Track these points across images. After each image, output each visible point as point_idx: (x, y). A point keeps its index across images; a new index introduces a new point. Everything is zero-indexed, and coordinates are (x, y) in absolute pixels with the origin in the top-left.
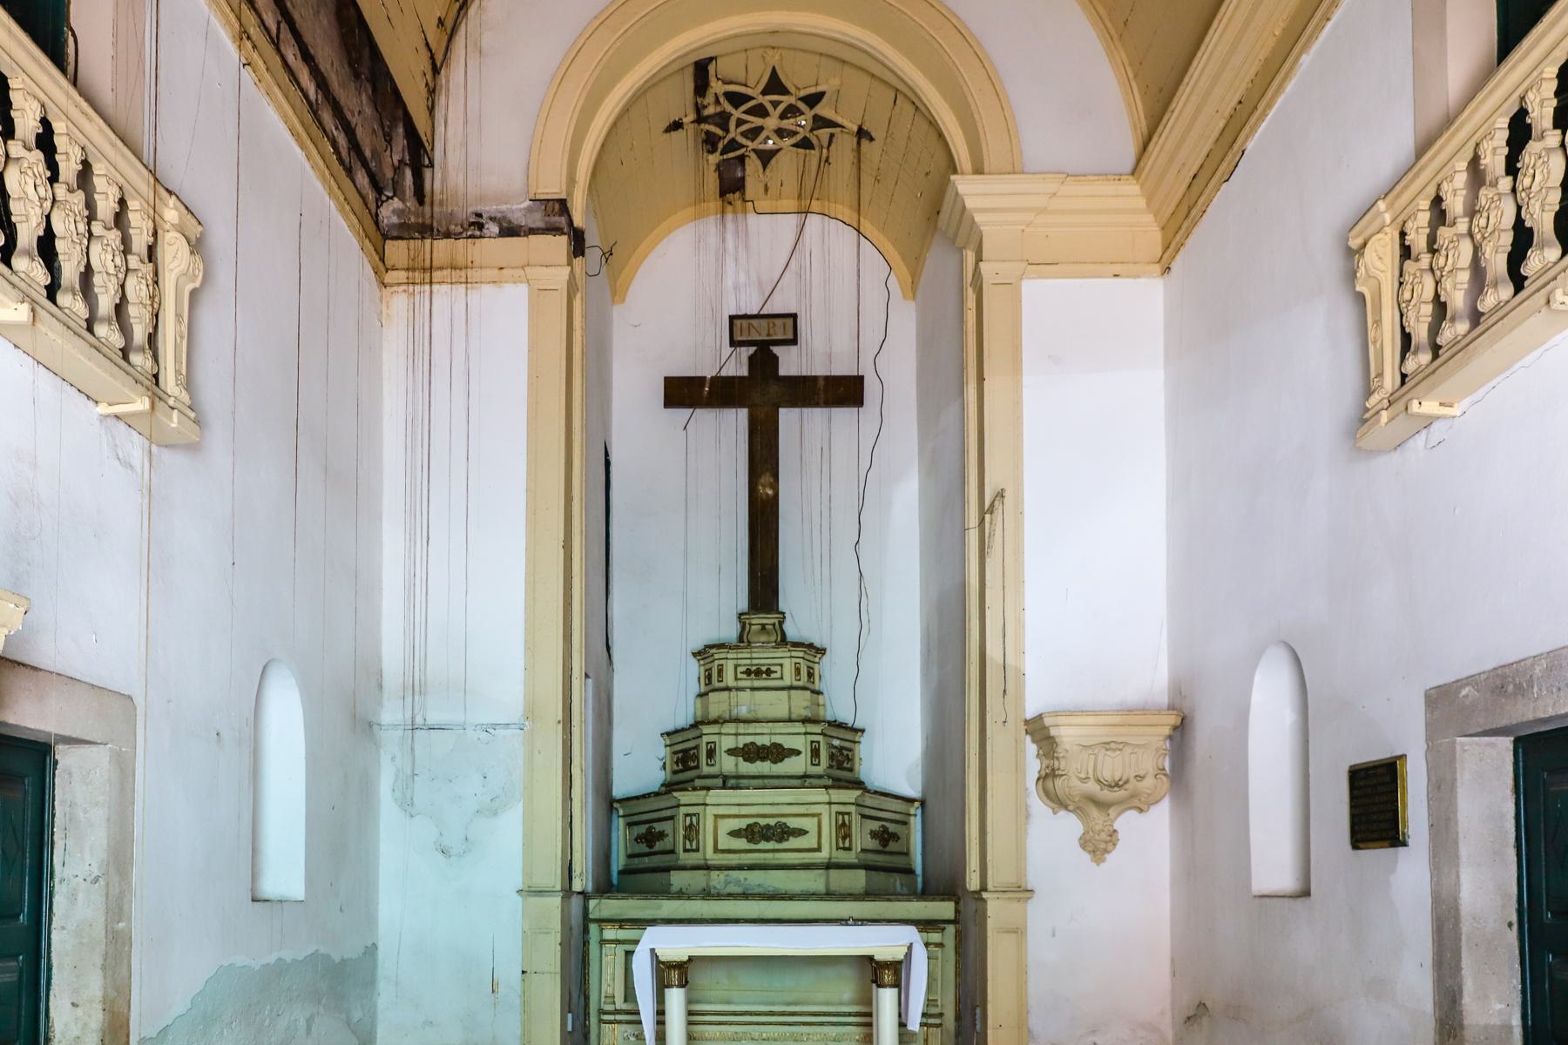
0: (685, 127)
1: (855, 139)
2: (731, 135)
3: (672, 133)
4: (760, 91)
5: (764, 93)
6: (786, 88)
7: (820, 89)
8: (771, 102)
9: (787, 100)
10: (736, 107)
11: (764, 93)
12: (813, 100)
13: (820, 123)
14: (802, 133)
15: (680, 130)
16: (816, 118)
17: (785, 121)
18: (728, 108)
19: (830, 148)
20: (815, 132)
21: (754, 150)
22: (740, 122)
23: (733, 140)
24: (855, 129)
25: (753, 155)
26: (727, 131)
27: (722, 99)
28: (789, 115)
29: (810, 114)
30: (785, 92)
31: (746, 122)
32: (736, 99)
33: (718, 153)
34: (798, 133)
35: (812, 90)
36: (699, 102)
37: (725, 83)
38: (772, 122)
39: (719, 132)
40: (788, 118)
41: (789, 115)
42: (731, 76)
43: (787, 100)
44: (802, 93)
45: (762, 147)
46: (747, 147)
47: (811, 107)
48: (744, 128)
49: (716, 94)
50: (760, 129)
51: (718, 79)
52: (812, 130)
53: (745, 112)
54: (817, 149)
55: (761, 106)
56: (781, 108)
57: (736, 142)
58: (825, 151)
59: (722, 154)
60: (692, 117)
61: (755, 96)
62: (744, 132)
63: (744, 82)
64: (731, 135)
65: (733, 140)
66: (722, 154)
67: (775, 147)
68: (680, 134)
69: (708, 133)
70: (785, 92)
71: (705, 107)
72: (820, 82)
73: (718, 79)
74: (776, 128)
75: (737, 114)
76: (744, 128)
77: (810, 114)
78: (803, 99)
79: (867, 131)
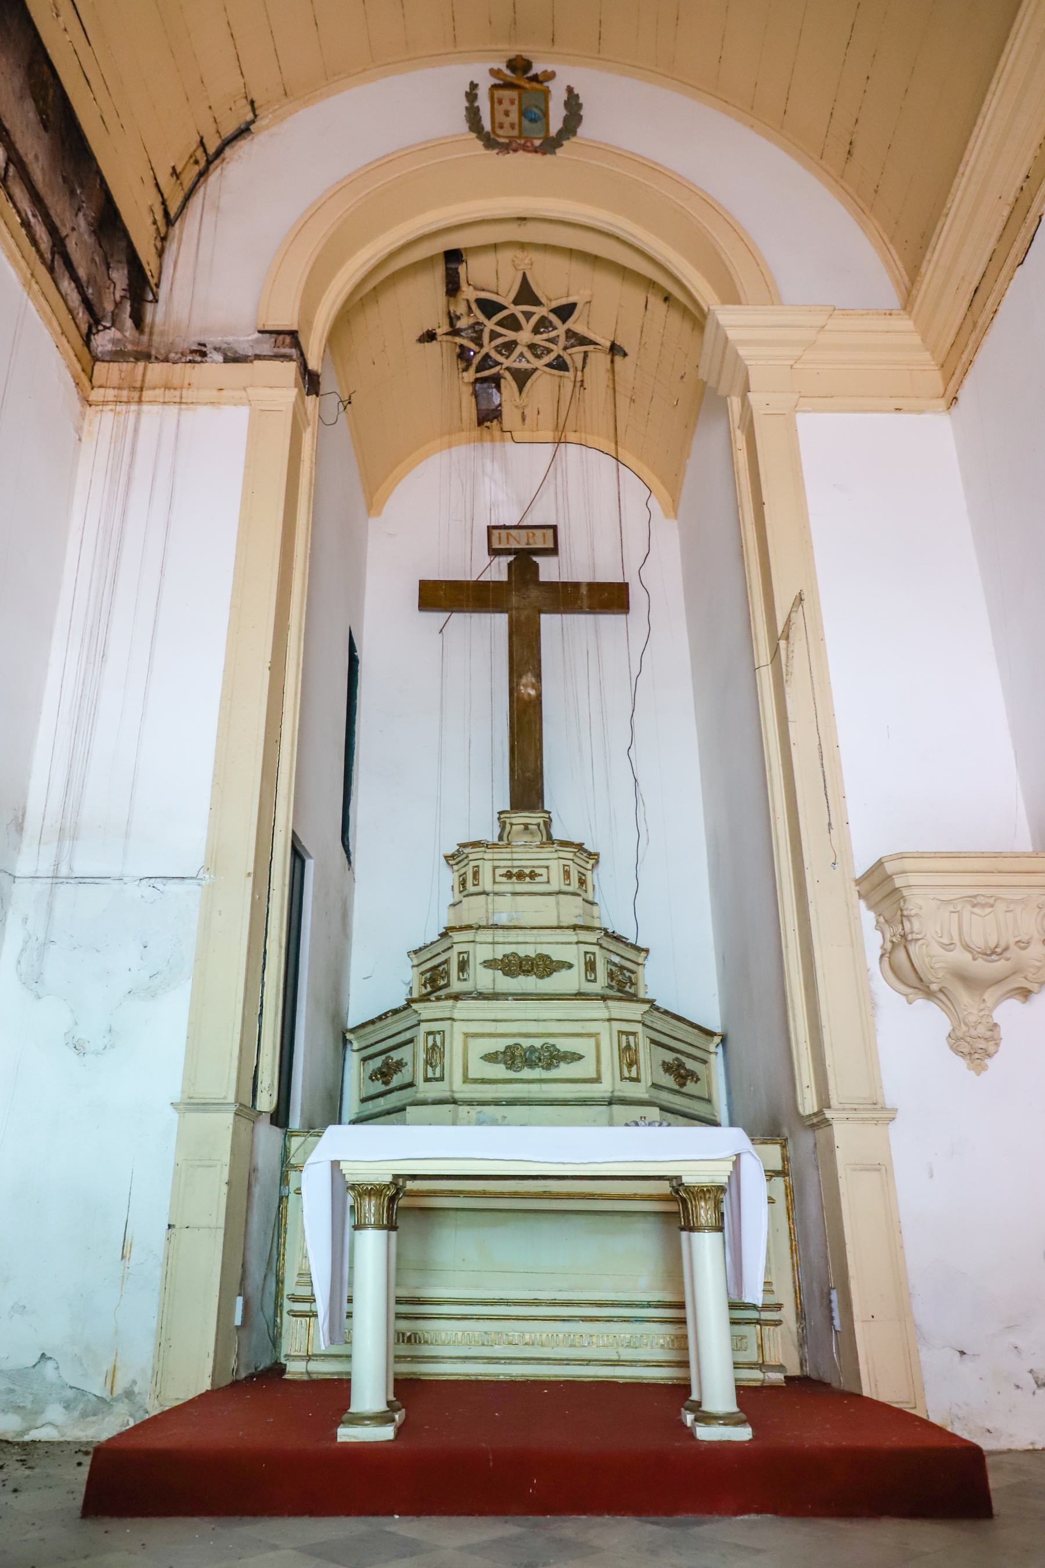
0: (439, 338)
1: (609, 357)
2: (484, 351)
3: (426, 344)
4: (511, 300)
5: (516, 302)
7: (571, 300)
8: (523, 312)
9: (540, 312)
10: (489, 318)
11: (516, 302)
12: (565, 312)
13: (573, 341)
14: (557, 350)
15: (434, 342)
16: (570, 334)
17: (539, 337)
18: (482, 318)
20: (569, 351)
21: (507, 369)
22: (494, 335)
23: (487, 356)
24: (608, 344)
26: (481, 346)
27: (474, 306)
28: (542, 330)
29: (561, 329)
30: (537, 302)
31: (501, 335)
32: (489, 308)
33: (473, 369)
34: (552, 351)
35: (564, 301)
36: (452, 311)
37: (476, 289)
38: (525, 336)
40: (541, 333)
41: (542, 330)
42: (480, 283)
43: (540, 312)
44: (554, 304)
45: (517, 365)
46: (502, 364)
47: (564, 322)
48: (499, 341)
49: (468, 301)
50: (514, 343)
51: (469, 285)
52: (565, 348)
53: (499, 323)
54: (571, 370)
55: (513, 316)
56: (534, 320)
57: (490, 357)
58: (579, 373)
59: (477, 371)
60: (446, 328)
61: (506, 304)
62: (497, 346)
63: (495, 290)
64: (484, 351)
65: (487, 356)
66: (477, 371)
69: (461, 346)
70: (537, 302)
71: (459, 318)
72: (570, 293)
73: (469, 285)
74: (529, 343)
76: (499, 341)
78: (554, 311)
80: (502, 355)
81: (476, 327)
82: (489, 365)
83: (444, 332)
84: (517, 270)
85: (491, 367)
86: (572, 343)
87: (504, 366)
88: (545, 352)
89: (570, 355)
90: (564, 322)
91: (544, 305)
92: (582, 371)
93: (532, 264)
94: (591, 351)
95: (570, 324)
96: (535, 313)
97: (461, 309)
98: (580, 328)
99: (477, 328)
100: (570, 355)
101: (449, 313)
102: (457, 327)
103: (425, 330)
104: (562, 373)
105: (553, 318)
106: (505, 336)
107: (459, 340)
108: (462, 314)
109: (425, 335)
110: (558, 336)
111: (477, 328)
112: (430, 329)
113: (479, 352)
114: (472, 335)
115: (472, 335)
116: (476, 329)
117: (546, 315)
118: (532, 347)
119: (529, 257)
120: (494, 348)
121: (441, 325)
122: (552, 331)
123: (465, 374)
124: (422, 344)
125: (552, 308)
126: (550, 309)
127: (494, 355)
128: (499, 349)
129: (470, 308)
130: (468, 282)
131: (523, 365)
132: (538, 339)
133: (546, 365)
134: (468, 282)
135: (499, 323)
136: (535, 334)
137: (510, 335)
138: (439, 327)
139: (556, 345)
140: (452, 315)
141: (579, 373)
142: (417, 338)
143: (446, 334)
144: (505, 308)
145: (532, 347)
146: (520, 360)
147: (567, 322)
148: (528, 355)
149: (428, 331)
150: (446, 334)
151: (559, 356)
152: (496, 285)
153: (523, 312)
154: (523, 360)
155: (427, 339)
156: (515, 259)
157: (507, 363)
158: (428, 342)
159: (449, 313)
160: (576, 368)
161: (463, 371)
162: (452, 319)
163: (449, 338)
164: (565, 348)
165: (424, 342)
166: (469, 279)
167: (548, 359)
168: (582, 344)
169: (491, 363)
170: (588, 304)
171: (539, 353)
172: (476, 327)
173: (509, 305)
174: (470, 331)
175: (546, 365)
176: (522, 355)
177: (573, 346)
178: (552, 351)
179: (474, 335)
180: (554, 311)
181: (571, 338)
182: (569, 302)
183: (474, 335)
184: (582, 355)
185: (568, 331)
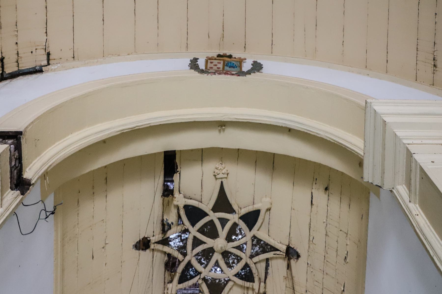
4: (211, 208)
5: (215, 209)
6: (230, 205)
7: (256, 207)
8: (219, 219)
9: (233, 218)
10: (193, 225)
11: (215, 209)
13: (257, 248)
15: (148, 251)
16: (256, 241)
18: (187, 224)
19: (267, 280)
20: (256, 259)
22: (197, 242)
23: (189, 265)
24: (284, 248)
26: (185, 255)
28: (234, 237)
30: (231, 210)
34: (241, 259)
35: (251, 209)
36: (165, 220)
37: (185, 197)
39: (176, 254)
40: (233, 241)
43: (233, 218)
44: (243, 212)
45: (212, 275)
46: (200, 273)
52: (252, 257)
53: (201, 231)
54: (256, 279)
55: (211, 222)
56: (228, 226)
57: (192, 266)
61: (208, 212)
62: (197, 254)
63: (199, 198)
64: (187, 258)
65: (189, 265)
68: (146, 255)
69: (169, 255)
70: (231, 210)
71: (170, 228)
72: (255, 202)
74: (224, 249)
75: (194, 231)
77: (249, 235)
78: (243, 218)
79: (293, 248)
80: (201, 264)
81: (183, 235)
82: (190, 275)
83: (157, 240)
84: (216, 179)
85: (192, 277)
86: (257, 251)
87: (202, 276)
88: (236, 261)
89: (255, 263)
90: (250, 229)
91: (236, 213)
92: (265, 283)
93: (228, 174)
94: (272, 258)
95: (254, 231)
96: (229, 220)
97: (172, 218)
98: (262, 235)
99: (184, 236)
100: (255, 263)
101: (163, 220)
102: (167, 236)
103: (141, 238)
104: (248, 284)
105: (242, 224)
106: (205, 243)
107: (166, 249)
108: (172, 223)
109: (141, 242)
110: (246, 244)
111: (184, 236)
112: (146, 236)
113: (183, 260)
114: (178, 244)
115: (178, 244)
116: (183, 238)
117: (237, 222)
118: (226, 254)
119: (226, 169)
120: (196, 255)
121: (155, 235)
122: (241, 238)
123: (170, 286)
124: (137, 251)
125: (242, 214)
126: (240, 216)
127: (195, 263)
128: (199, 257)
129: (179, 217)
130: (179, 191)
132: (229, 247)
133: (235, 275)
134: (179, 191)
135: (201, 231)
136: (228, 242)
137: (209, 242)
138: (153, 236)
139: (244, 253)
140: (165, 222)
141: (262, 284)
142: (134, 243)
143: (158, 243)
144: (206, 215)
145: (226, 254)
146: (216, 270)
147: (253, 230)
148: (222, 263)
149: (145, 238)
150: (158, 243)
151: (247, 265)
152: (201, 198)
153: (219, 219)
154: (218, 269)
155: (142, 247)
156: (217, 171)
157: (206, 273)
158: (143, 250)
159: (163, 220)
160: (260, 279)
161: (168, 283)
163: (160, 247)
164: (252, 257)
165: (139, 250)
166: (181, 189)
167: (237, 268)
168: (264, 252)
169: (192, 273)
170: (268, 212)
171: (231, 261)
172: (183, 235)
173: (209, 211)
174: (177, 240)
175: (235, 275)
176: (217, 264)
177: (257, 254)
178: (241, 259)
179: (181, 244)
180: (243, 218)
181: (256, 245)
182: (254, 209)
183: (181, 244)
184: (264, 264)
185: (254, 237)
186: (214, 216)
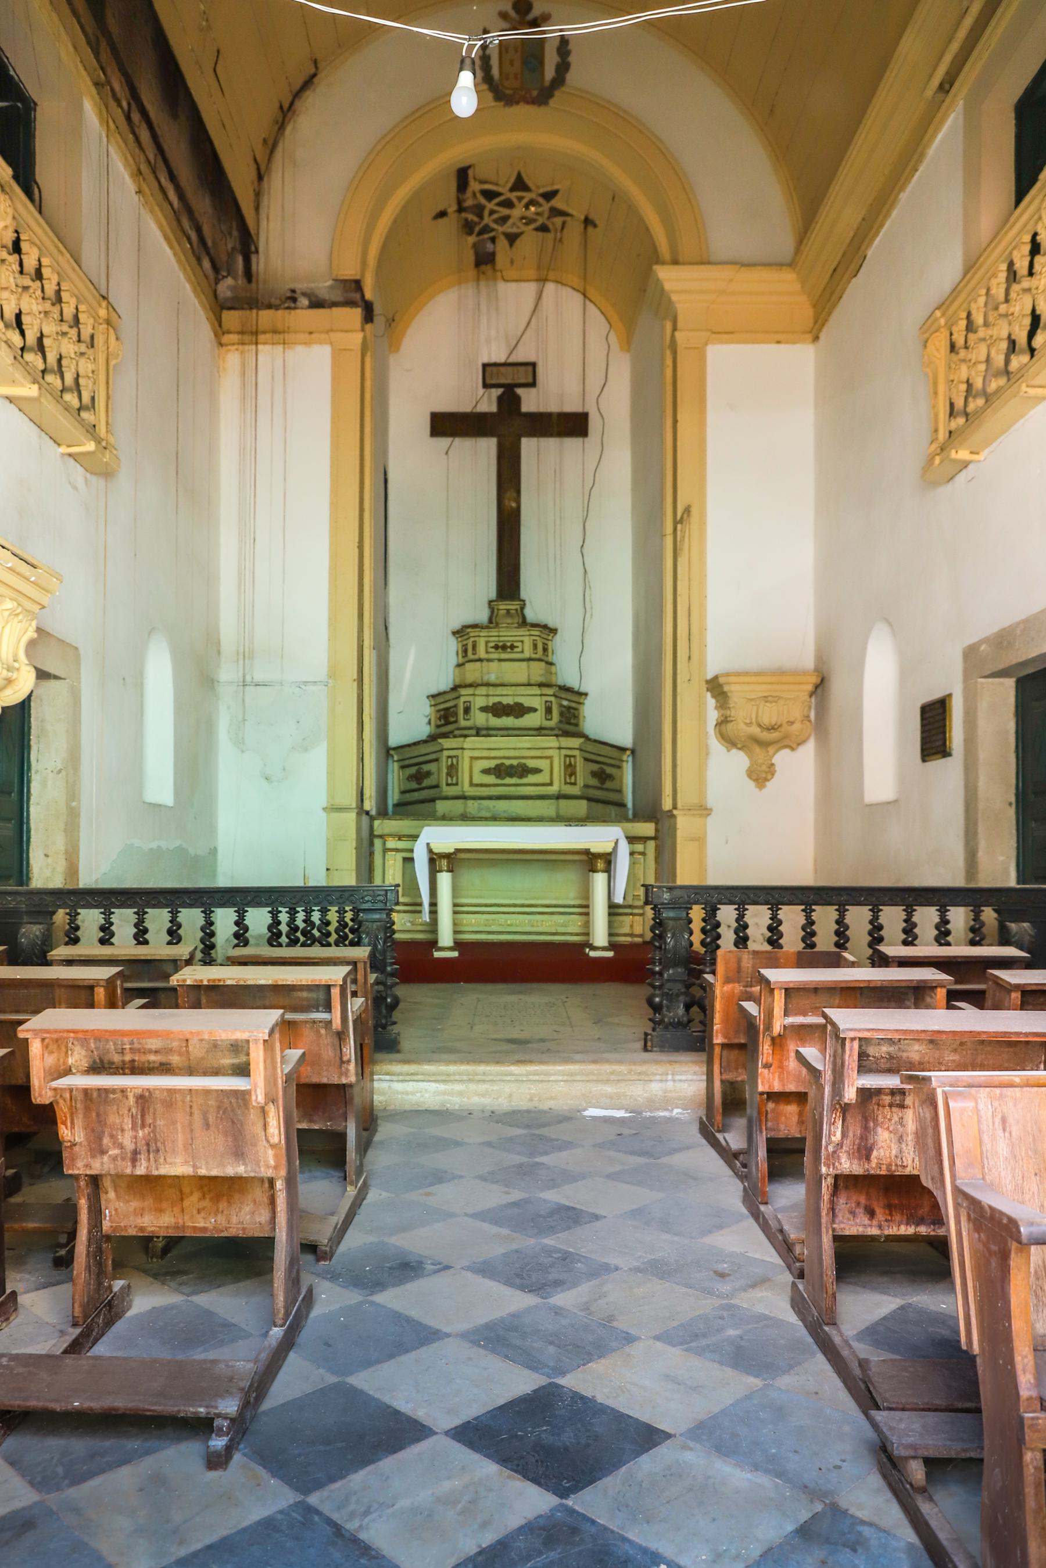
5: (512, 190)
7: (555, 187)
11: (512, 190)
12: (549, 196)
14: (540, 221)
18: (482, 201)
22: (492, 212)
23: (487, 225)
24: (583, 218)
25: (502, 237)
26: (481, 217)
27: (478, 195)
32: (489, 195)
35: (549, 189)
38: (517, 212)
43: (528, 196)
44: (542, 191)
45: (510, 230)
48: (495, 216)
56: (525, 201)
58: (559, 234)
60: (455, 207)
67: (519, 231)
75: (490, 206)
131: (514, 230)
141: (559, 234)
162: (459, 203)
186: (513, 196)
